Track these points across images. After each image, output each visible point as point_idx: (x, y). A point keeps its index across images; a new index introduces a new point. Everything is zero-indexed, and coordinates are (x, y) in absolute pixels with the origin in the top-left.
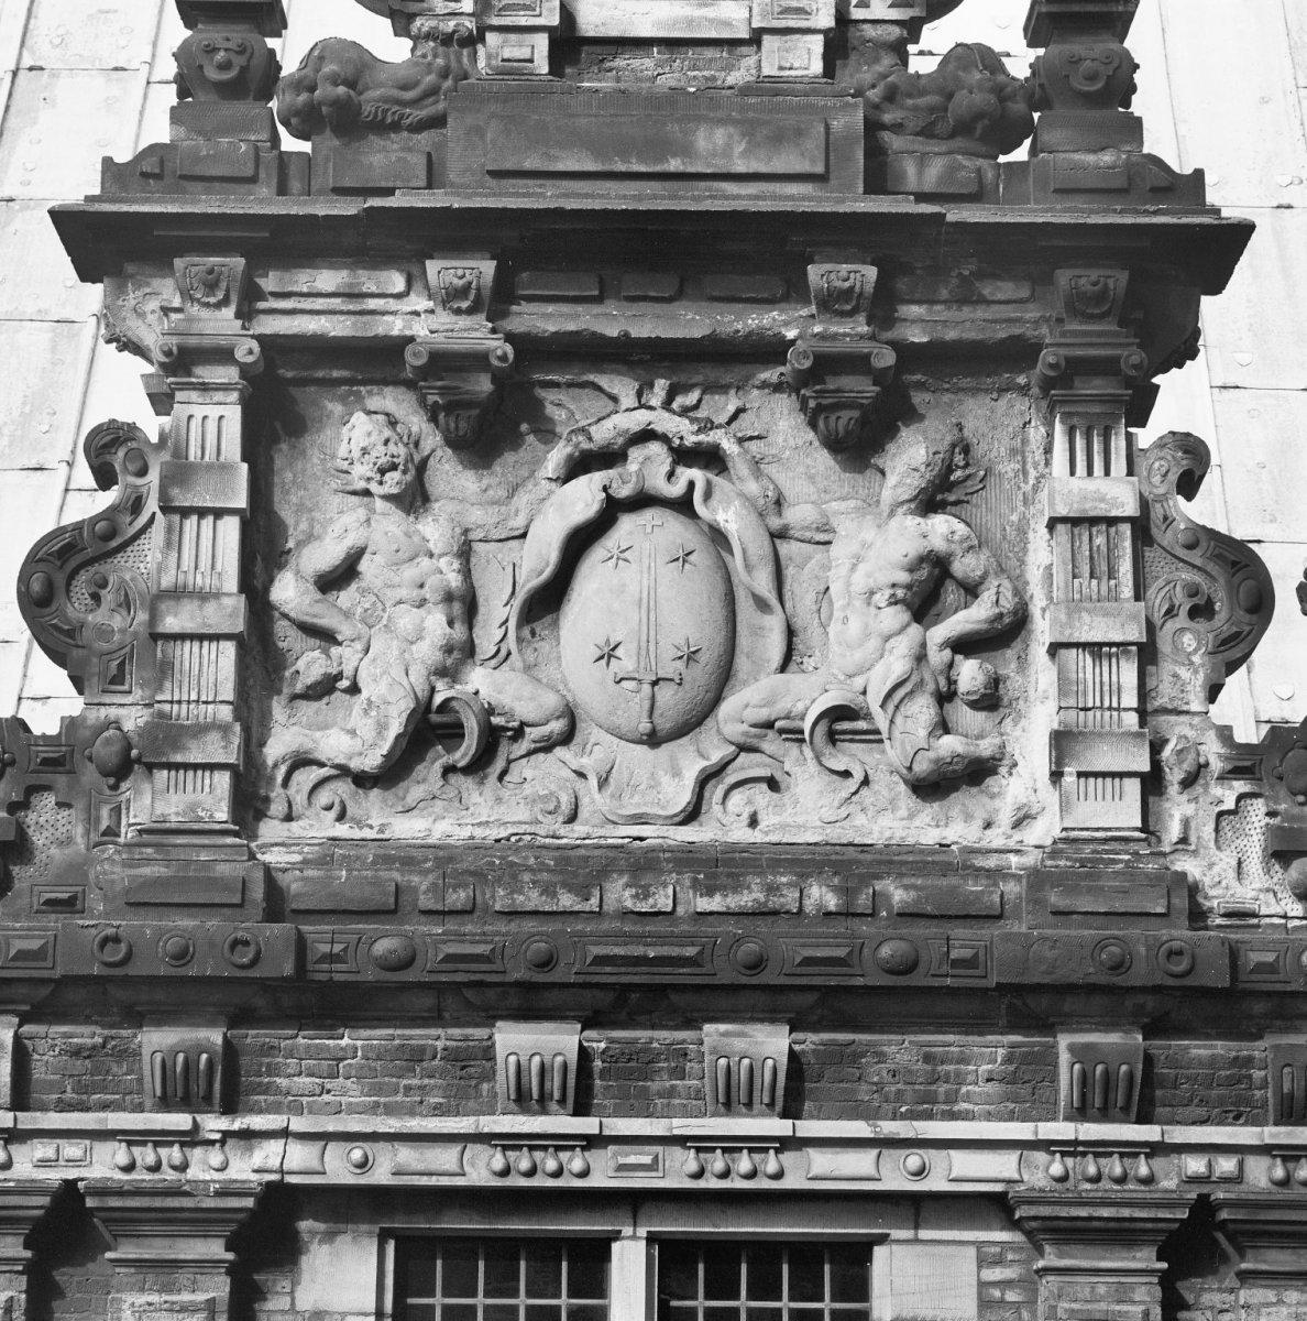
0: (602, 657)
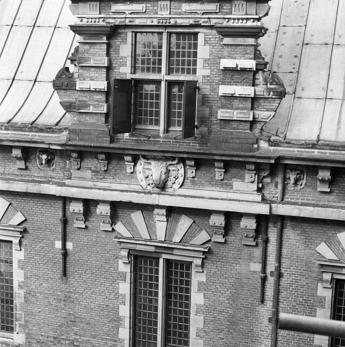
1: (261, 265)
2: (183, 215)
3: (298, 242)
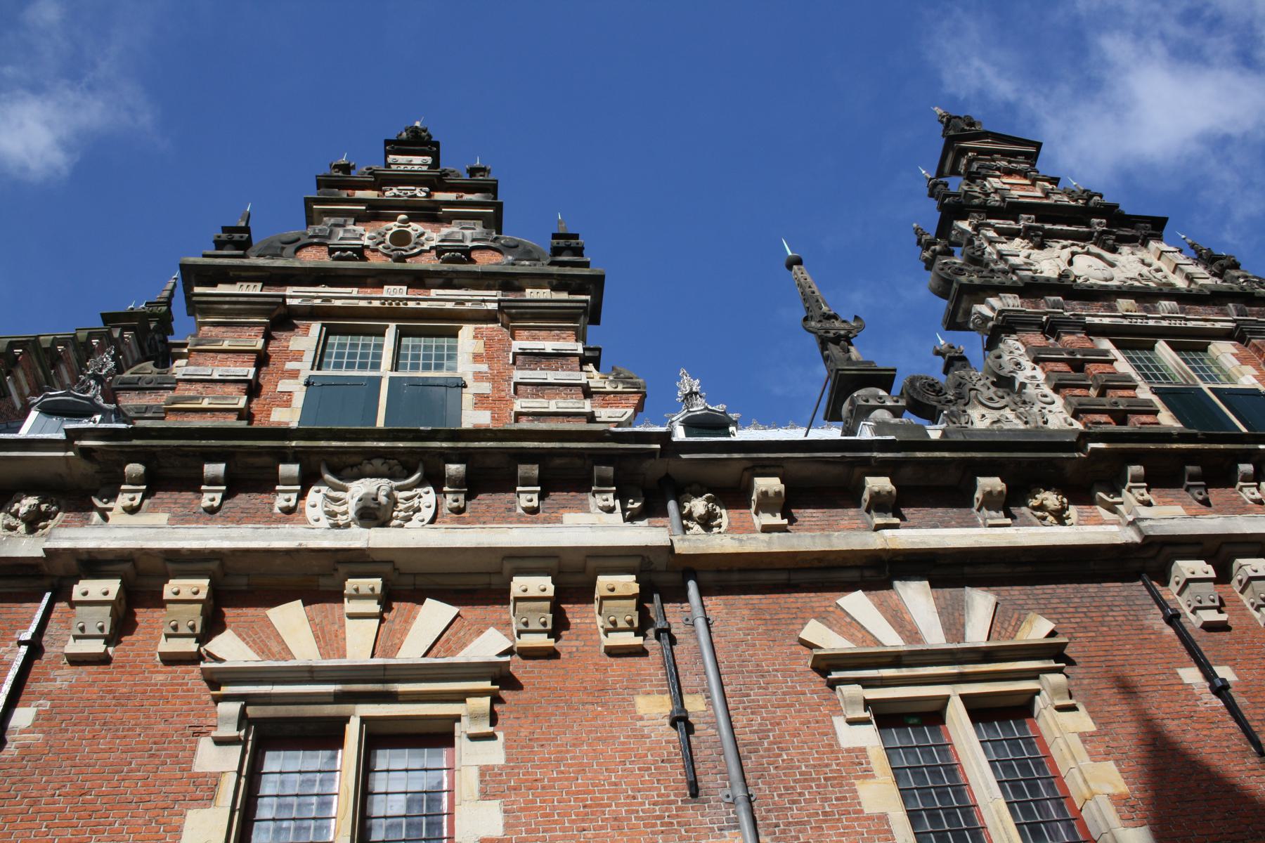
1: (667, 697)
2: (428, 601)
3: (749, 635)
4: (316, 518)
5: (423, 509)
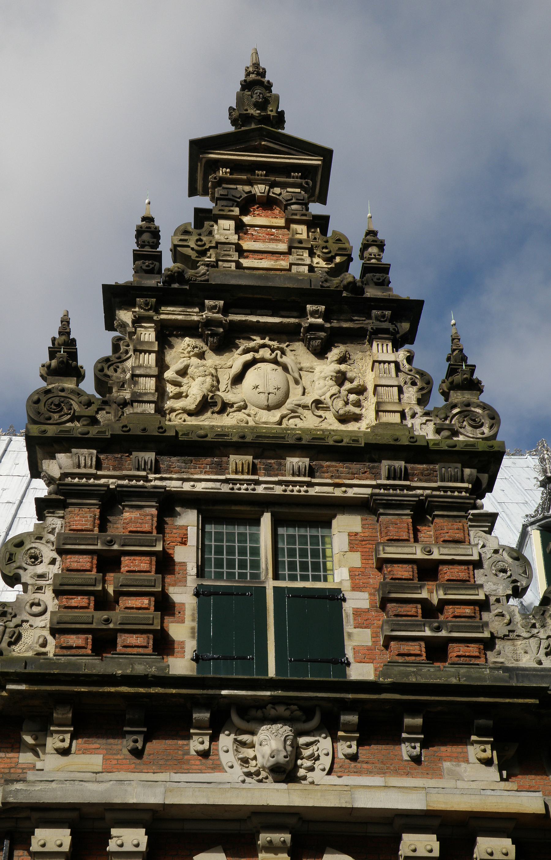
0: (254, 388)
4: (230, 764)
5: (322, 757)
